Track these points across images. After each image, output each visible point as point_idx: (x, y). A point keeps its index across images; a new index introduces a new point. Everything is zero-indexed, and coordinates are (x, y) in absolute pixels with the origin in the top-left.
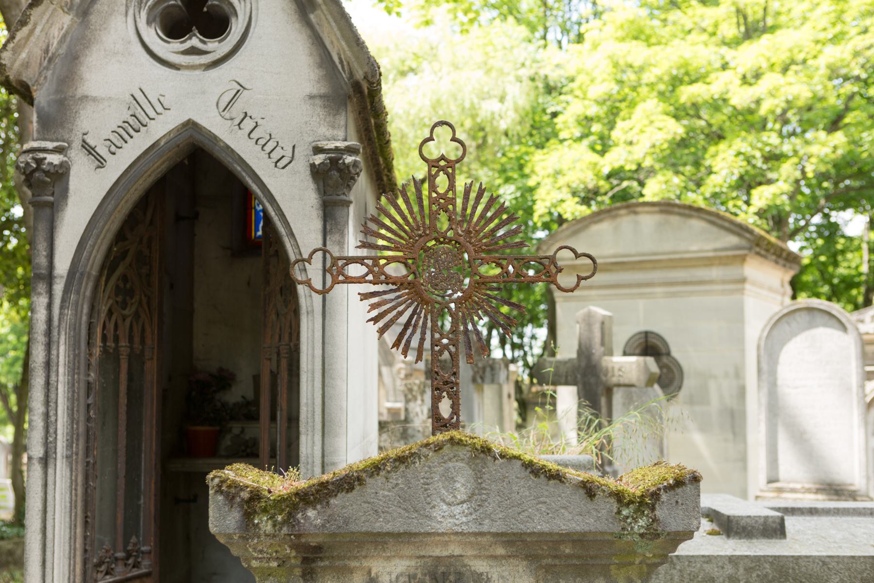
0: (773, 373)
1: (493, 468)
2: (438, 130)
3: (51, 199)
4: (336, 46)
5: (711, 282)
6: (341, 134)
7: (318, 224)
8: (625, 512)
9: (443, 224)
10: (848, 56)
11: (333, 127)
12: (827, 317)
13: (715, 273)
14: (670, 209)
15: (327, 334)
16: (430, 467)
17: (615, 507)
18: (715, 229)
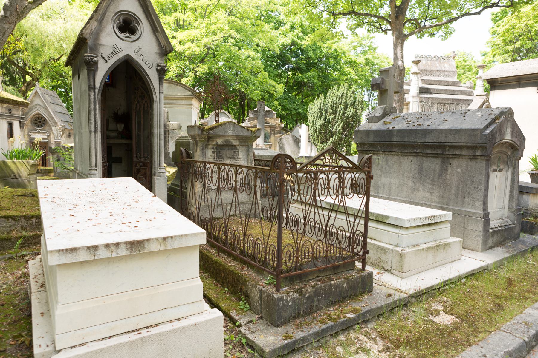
5: (183, 104)
6: (163, 62)
7: (158, 82)
10: (210, 41)
13: (184, 102)
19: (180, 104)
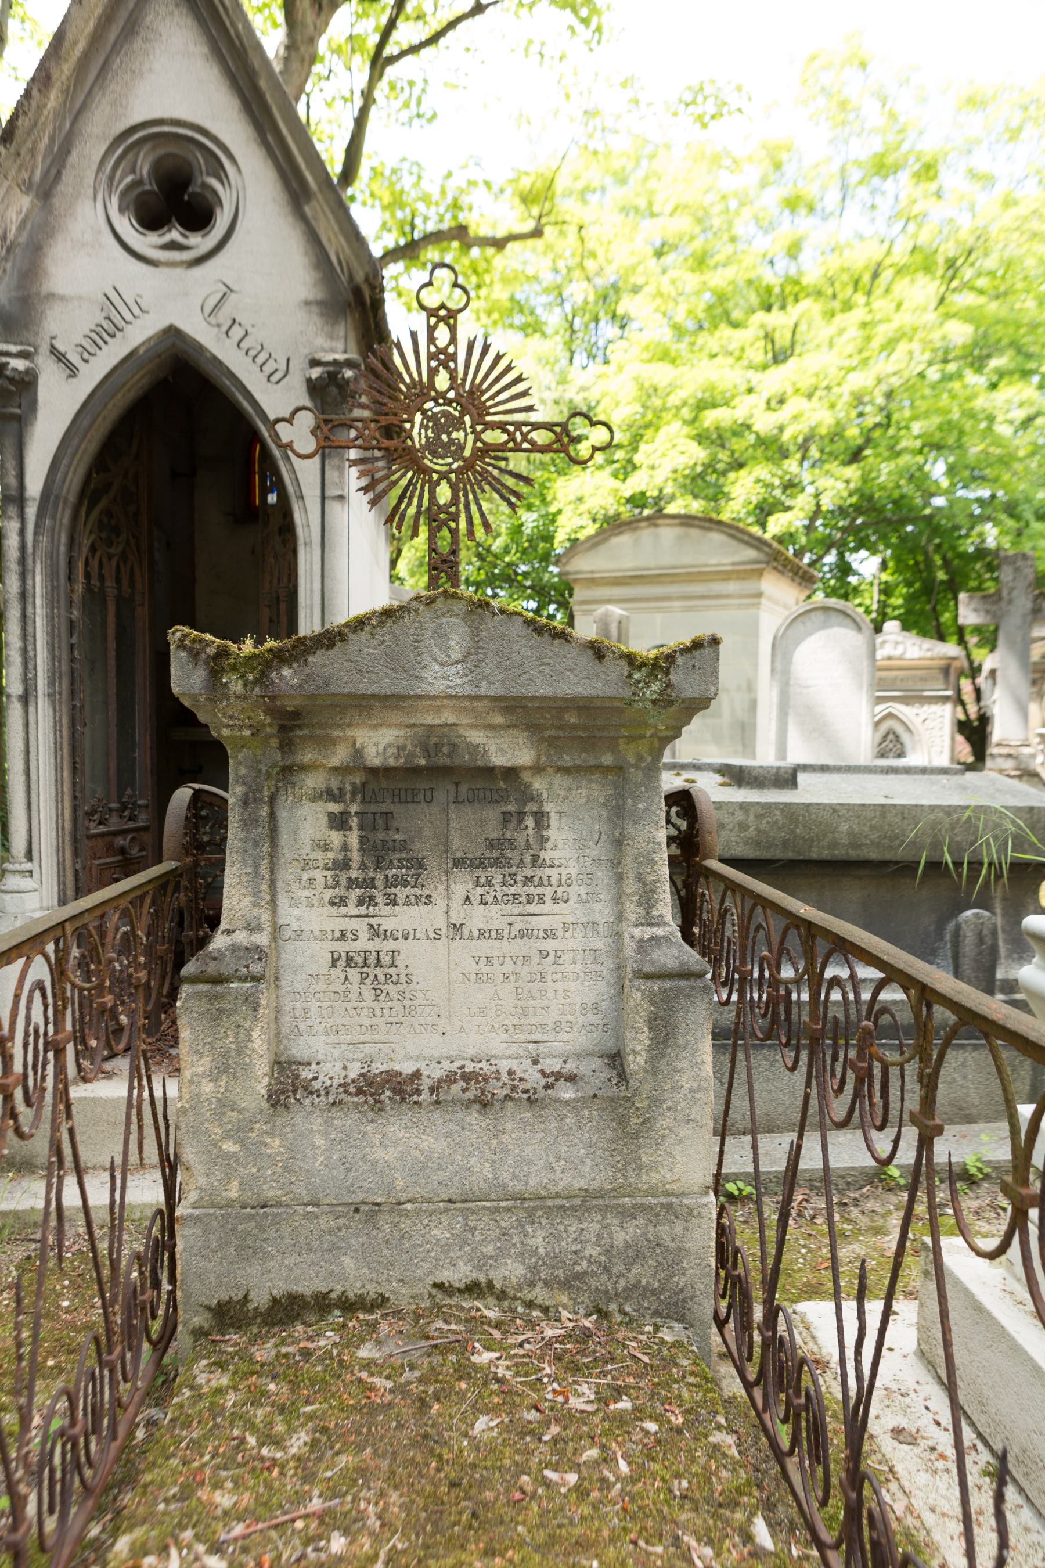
0: (788, 661)
1: (492, 625)
2: (438, 272)
3: (18, 411)
4: (334, 244)
5: (728, 596)
6: (340, 346)
8: (637, 676)
9: (442, 381)
10: (870, 382)
11: (332, 338)
12: (841, 617)
14: (690, 521)
15: (326, 566)
16: (420, 622)
17: (626, 670)
18: (734, 543)
19: (718, 596)
